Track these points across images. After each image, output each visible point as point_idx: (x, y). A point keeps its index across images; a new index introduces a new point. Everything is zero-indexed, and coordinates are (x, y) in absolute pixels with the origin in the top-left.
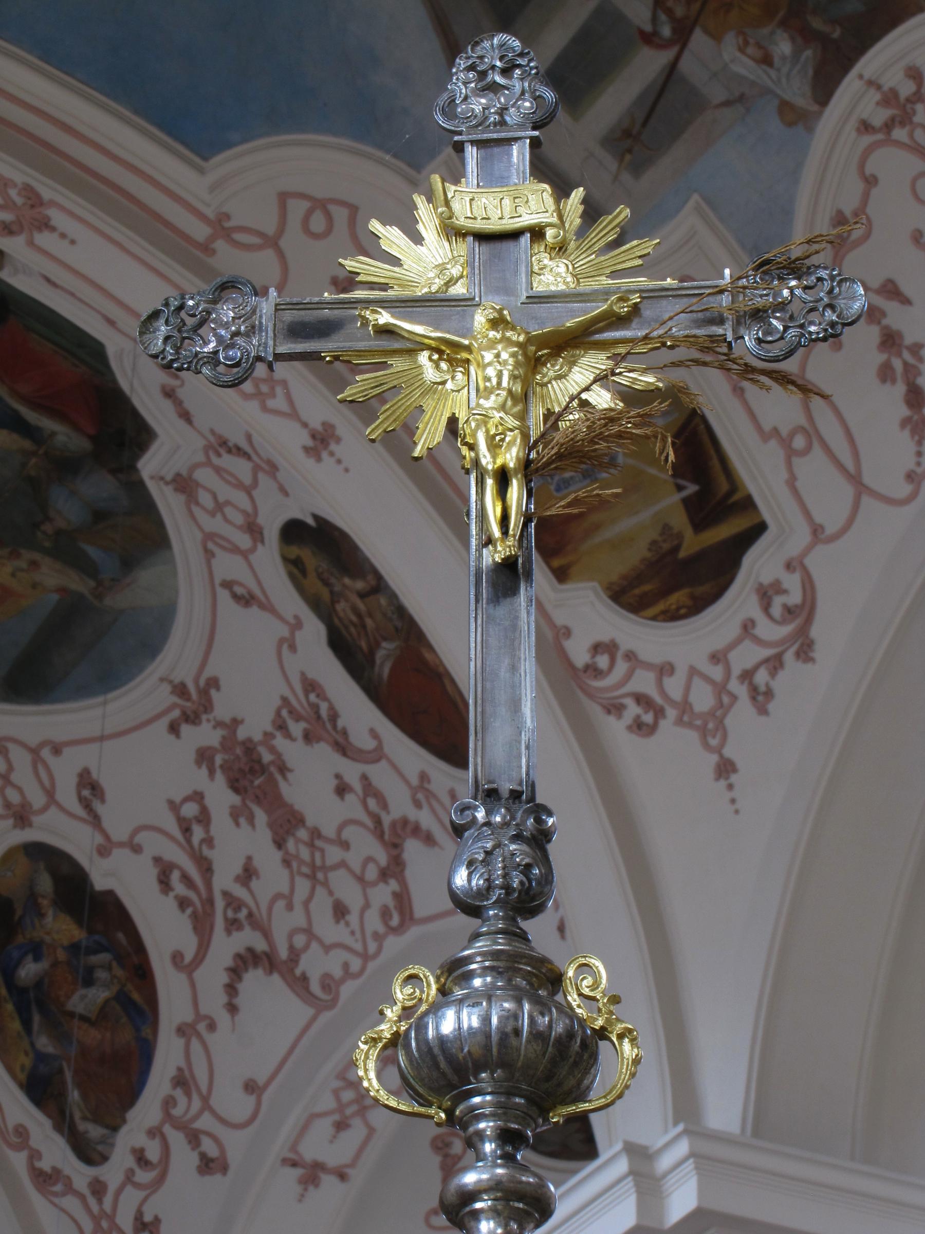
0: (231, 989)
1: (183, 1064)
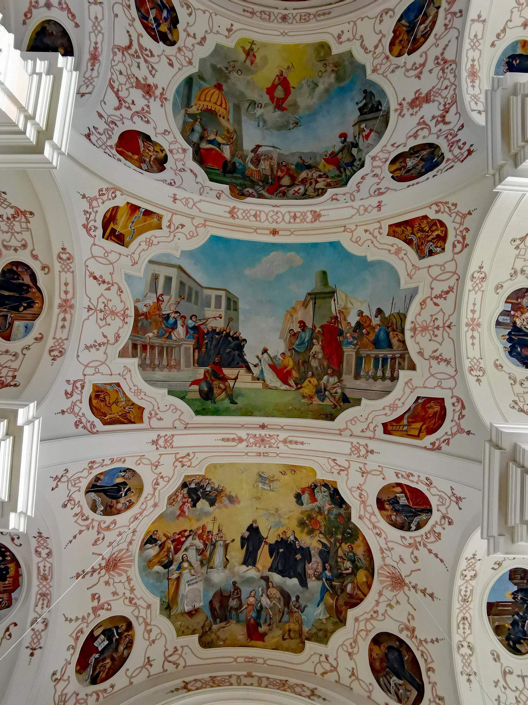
0: (130, 36)
1: (131, 11)
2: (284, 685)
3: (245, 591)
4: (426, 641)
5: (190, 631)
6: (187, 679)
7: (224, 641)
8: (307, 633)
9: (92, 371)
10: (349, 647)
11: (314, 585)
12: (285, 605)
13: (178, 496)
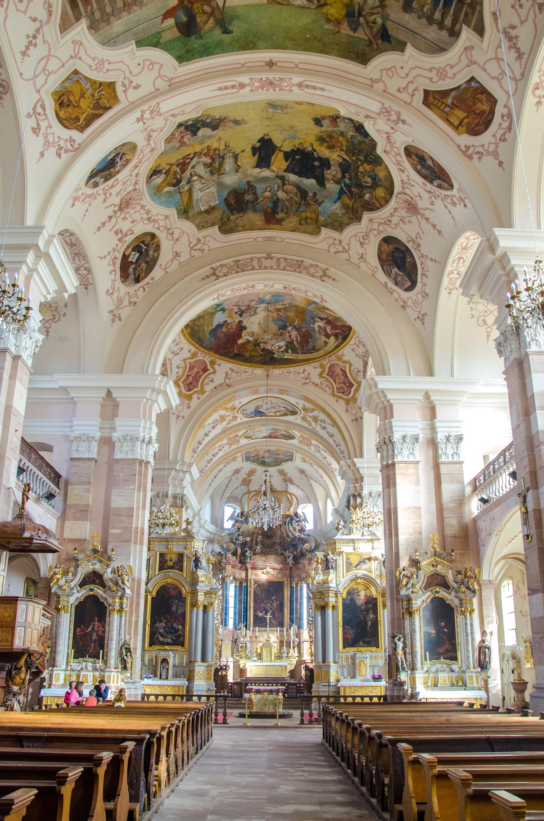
2: (300, 266)
3: (260, 188)
4: (427, 256)
5: (209, 225)
6: (214, 266)
7: (243, 227)
8: (323, 221)
9: (42, 77)
10: (361, 238)
11: (332, 187)
12: (301, 199)
13: (174, 135)
